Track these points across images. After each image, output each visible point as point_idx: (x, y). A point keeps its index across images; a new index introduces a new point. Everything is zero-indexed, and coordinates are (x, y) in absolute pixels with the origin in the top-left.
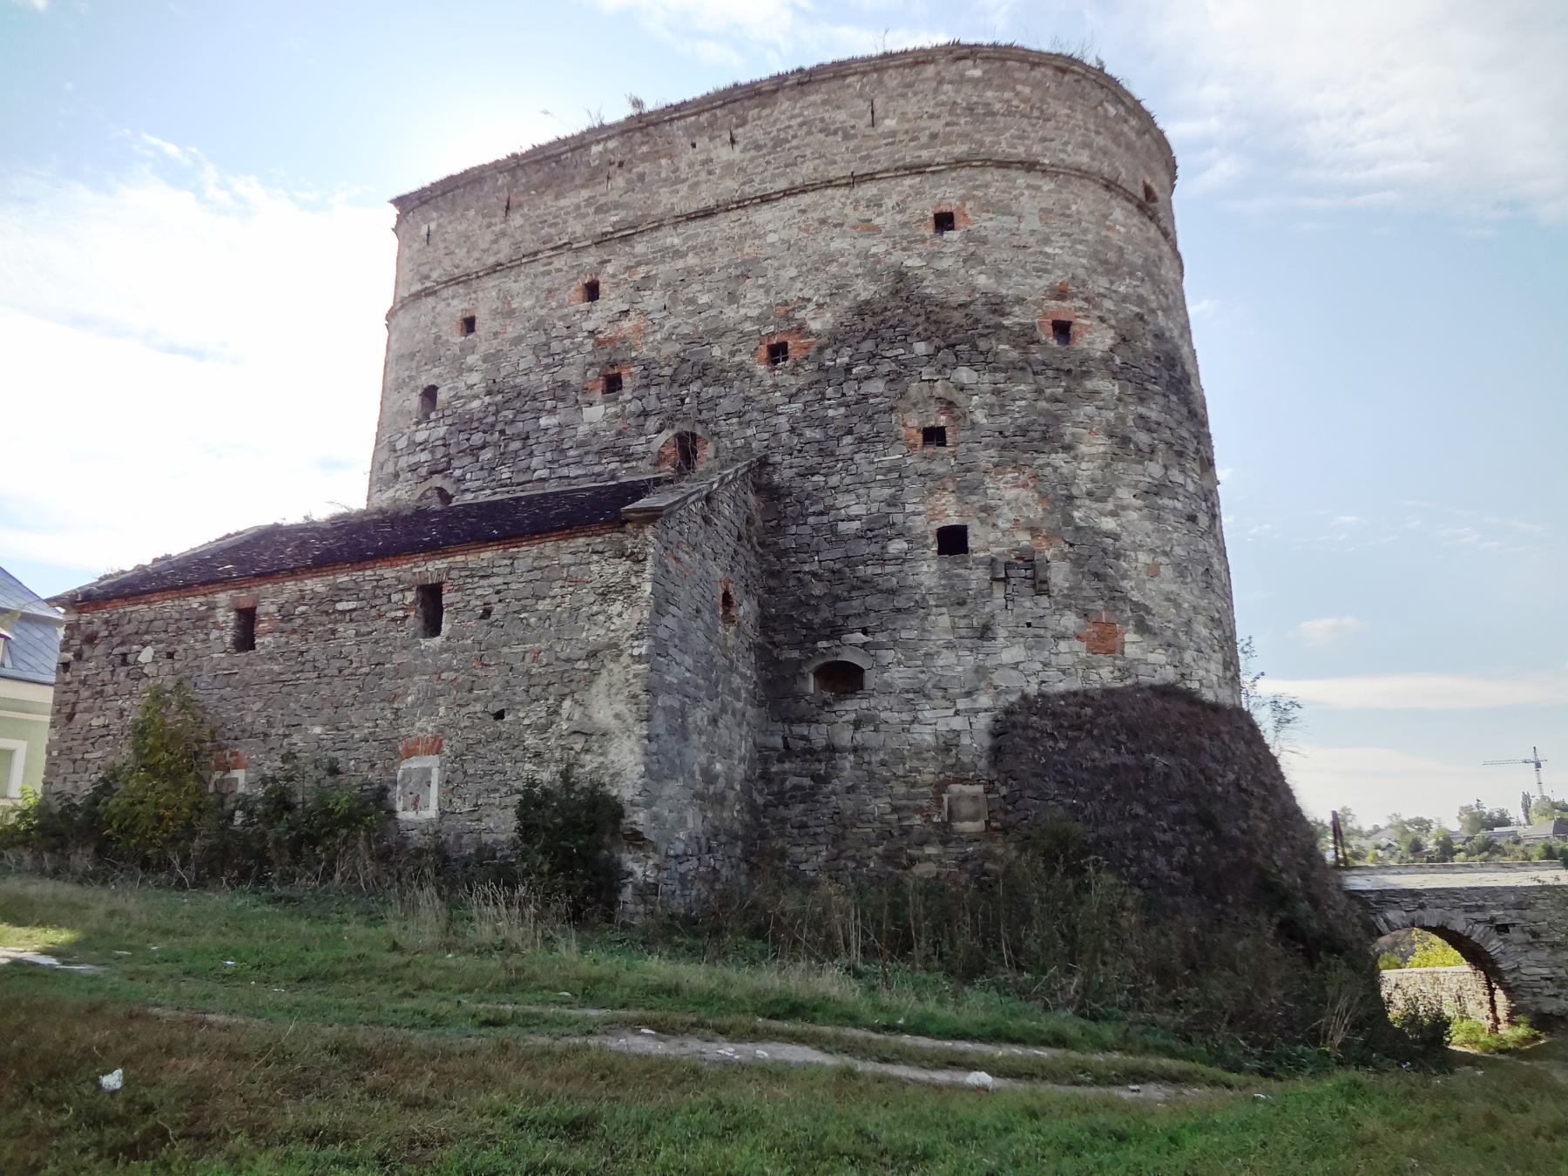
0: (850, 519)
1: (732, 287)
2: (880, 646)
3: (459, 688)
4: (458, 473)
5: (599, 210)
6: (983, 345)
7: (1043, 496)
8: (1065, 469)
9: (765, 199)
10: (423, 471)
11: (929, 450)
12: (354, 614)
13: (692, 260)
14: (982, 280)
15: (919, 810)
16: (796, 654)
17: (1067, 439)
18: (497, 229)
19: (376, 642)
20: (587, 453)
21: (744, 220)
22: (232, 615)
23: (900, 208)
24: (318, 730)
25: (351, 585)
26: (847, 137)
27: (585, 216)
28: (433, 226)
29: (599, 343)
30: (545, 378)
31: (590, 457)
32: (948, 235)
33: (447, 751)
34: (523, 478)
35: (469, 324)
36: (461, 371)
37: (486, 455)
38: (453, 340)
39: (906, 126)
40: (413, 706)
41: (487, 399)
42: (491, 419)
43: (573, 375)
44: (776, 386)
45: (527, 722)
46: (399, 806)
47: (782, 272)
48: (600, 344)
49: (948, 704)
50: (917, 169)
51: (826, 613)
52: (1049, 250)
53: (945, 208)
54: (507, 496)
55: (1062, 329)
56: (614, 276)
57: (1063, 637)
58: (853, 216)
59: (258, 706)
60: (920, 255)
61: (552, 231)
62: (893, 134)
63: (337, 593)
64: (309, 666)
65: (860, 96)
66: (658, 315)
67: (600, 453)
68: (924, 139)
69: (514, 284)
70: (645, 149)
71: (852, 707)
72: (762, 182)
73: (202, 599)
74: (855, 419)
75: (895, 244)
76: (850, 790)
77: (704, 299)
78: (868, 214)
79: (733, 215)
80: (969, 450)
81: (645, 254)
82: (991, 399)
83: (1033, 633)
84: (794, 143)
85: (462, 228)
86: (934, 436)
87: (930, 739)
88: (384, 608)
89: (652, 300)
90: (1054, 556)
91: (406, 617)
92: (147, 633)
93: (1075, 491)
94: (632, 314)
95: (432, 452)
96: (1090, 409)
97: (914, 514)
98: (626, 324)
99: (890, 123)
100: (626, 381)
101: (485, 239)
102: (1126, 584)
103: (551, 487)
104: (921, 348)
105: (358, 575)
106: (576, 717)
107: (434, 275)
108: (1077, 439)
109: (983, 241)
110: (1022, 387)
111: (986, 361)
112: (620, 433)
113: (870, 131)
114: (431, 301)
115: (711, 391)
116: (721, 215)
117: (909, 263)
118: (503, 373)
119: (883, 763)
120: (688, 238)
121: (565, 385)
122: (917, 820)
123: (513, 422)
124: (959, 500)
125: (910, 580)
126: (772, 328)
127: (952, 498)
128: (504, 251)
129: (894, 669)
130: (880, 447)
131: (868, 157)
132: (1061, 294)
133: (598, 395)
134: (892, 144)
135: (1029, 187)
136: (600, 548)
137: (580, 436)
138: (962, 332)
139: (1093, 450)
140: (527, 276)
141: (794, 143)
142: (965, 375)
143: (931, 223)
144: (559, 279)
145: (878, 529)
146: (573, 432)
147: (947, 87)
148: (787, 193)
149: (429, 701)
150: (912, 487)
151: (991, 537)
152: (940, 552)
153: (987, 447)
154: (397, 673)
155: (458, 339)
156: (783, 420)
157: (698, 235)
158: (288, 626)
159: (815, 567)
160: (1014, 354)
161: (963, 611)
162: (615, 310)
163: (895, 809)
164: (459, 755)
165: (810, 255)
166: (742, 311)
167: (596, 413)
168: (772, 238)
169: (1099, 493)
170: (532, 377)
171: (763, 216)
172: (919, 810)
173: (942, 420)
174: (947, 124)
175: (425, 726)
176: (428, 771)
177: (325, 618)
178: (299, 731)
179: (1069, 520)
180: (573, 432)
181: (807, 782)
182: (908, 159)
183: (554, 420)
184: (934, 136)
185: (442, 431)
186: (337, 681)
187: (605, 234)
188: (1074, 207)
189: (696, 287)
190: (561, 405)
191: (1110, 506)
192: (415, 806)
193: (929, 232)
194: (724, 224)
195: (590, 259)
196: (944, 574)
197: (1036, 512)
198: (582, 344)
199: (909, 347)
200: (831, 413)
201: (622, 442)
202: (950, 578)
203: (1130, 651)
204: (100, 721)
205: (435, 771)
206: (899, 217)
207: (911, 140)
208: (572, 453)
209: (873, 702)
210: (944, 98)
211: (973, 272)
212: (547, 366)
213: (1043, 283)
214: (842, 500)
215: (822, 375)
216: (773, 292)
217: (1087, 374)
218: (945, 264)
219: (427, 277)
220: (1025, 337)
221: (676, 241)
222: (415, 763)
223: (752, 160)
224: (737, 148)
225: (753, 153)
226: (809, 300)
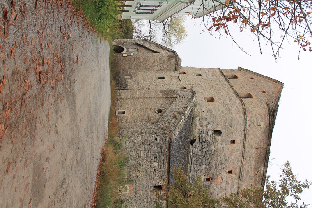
5: (248, 171)
10: (201, 136)
20: (194, 176)
22: (161, 185)
27: (248, 168)
29: (217, 176)
30: (214, 165)
35: (233, 142)
37: (200, 153)
43: (213, 171)
54: (189, 160)
59: (142, 194)
61: (248, 160)
64: (148, 204)
69: (238, 154)
73: (166, 177)
89: (224, 184)
92: (161, 163)
98: (220, 179)
101: (252, 143)
107: (249, 129)
133: (206, 177)
140: (239, 156)
146: (200, 173)
155: (231, 139)
183: (203, 168)
185: (209, 139)
198: (219, 172)
204: (142, 154)
208: (195, 173)
212: (216, 165)
219: (250, 126)
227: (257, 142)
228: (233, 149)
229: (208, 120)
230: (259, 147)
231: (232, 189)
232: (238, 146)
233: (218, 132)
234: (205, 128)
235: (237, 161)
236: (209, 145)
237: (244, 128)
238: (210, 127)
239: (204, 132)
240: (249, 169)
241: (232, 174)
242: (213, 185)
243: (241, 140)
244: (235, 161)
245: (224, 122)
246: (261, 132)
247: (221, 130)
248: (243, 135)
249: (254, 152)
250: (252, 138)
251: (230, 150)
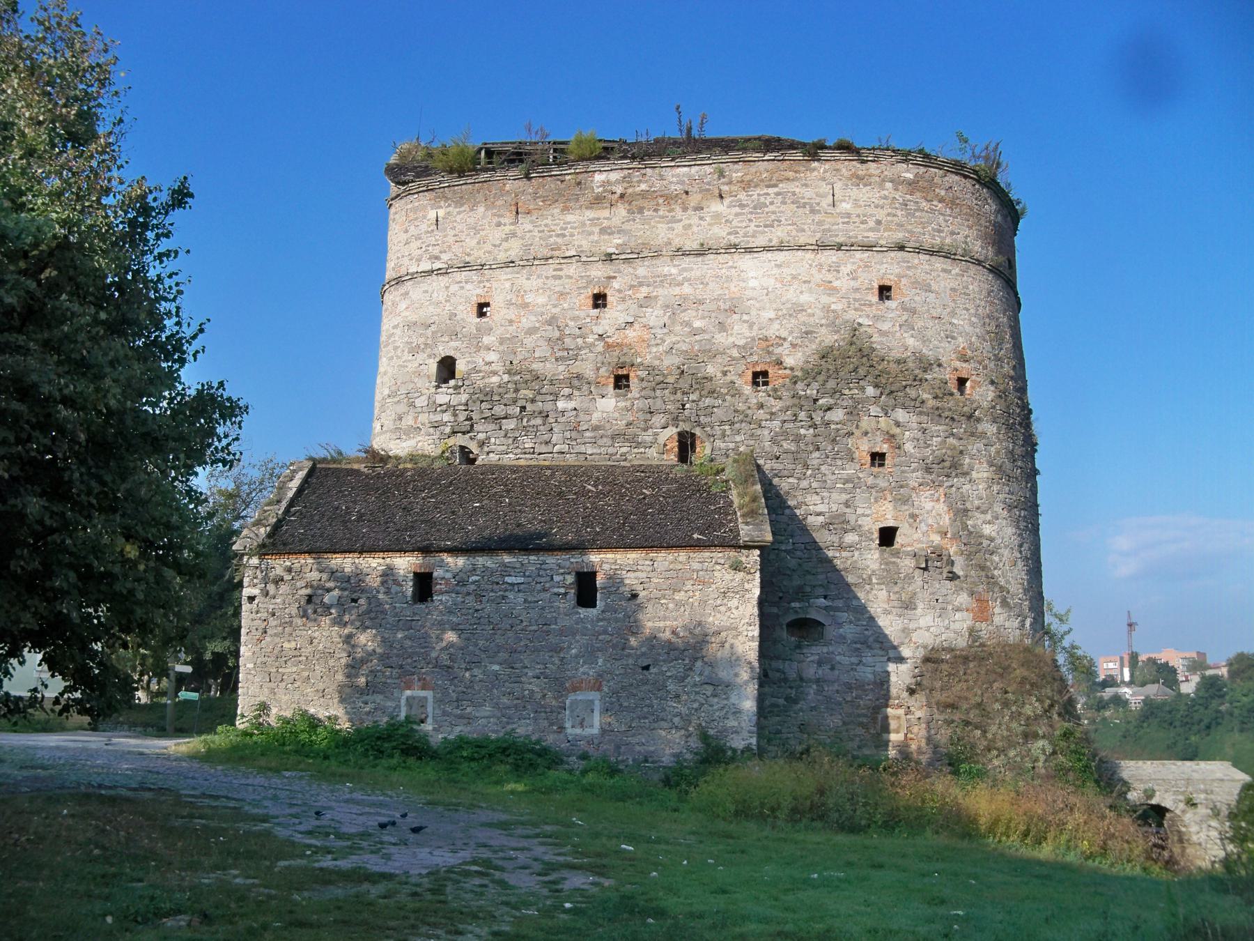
0: (819, 514)
1: (722, 318)
2: (837, 609)
3: (614, 647)
4: (481, 436)
5: (603, 231)
7: (950, 507)
9: (749, 250)
10: (448, 430)
11: (876, 470)
12: (522, 587)
13: (687, 289)
14: (911, 342)
15: (861, 724)
16: (775, 610)
17: (966, 467)
18: (508, 229)
19: (543, 608)
21: (730, 264)
23: (853, 276)
24: (496, 667)
25: (518, 565)
26: (813, 211)
27: (593, 233)
28: (441, 213)
29: (608, 346)
31: (605, 440)
32: (888, 303)
33: (606, 689)
34: (544, 449)
36: (478, 349)
37: (509, 425)
38: (469, 320)
39: (859, 211)
40: (577, 656)
41: (506, 378)
42: (511, 395)
44: (761, 406)
45: (669, 674)
46: (568, 725)
47: (762, 313)
48: (608, 346)
49: (881, 653)
50: (868, 247)
51: (797, 582)
52: (955, 321)
55: (962, 382)
56: (619, 291)
57: (958, 610)
58: (818, 277)
60: (868, 316)
61: (559, 240)
62: (849, 215)
63: (506, 569)
65: (824, 179)
66: (659, 331)
67: (613, 438)
68: (872, 224)
70: (643, 187)
71: (814, 653)
72: (745, 235)
73: (381, 561)
74: (821, 439)
75: (849, 303)
76: (812, 709)
77: (697, 324)
78: (829, 277)
80: (903, 472)
81: (645, 277)
83: (941, 607)
84: (772, 208)
85: (471, 221)
86: (877, 458)
87: (871, 676)
88: (547, 585)
89: (654, 316)
90: (956, 553)
91: (566, 594)
93: (968, 505)
94: (636, 326)
95: (455, 415)
97: (864, 515)
98: (631, 334)
99: (845, 206)
100: (633, 382)
101: (497, 235)
102: (996, 573)
103: (571, 459)
104: (870, 391)
105: (523, 559)
106: (706, 673)
107: (445, 257)
109: (913, 312)
110: (941, 428)
111: (917, 405)
112: (629, 424)
113: (830, 209)
115: (708, 401)
117: (860, 320)
118: (520, 357)
119: (837, 692)
120: (685, 270)
121: (579, 377)
122: (860, 731)
123: (533, 401)
124: (895, 508)
125: (859, 565)
126: (755, 358)
127: (890, 506)
128: (514, 249)
129: (847, 626)
130: (839, 463)
134: (848, 223)
135: (944, 270)
136: (722, 561)
137: (594, 422)
138: (896, 381)
139: (980, 475)
141: (772, 208)
142: (900, 415)
143: (877, 292)
144: (568, 285)
145: (838, 523)
146: (588, 418)
147: (889, 185)
148: (767, 249)
149: (589, 655)
150: (860, 495)
151: (916, 536)
152: (880, 545)
153: (913, 471)
154: (562, 633)
156: (766, 432)
157: (692, 269)
158: (464, 589)
159: (790, 547)
160: (931, 403)
161: (896, 589)
163: (844, 723)
164: (615, 692)
166: (731, 340)
167: (608, 405)
168: (753, 283)
169: (983, 508)
170: (548, 365)
171: (746, 263)
172: (861, 724)
173: (885, 448)
174: (889, 215)
175: (586, 671)
176: (592, 702)
177: (495, 587)
178: (479, 667)
179: (965, 527)
180: (588, 418)
181: (781, 701)
182: (860, 238)
183: (571, 405)
184: (879, 222)
185: (464, 397)
186: (510, 634)
189: (691, 313)
190: (576, 393)
191: (989, 517)
192: (582, 725)
193: (875, 299)
196: (883, 561)
197: (946, 520)
198: (593, 345)
200: (802, 431)
201: (631, 431)
202: (887, 564)
203: (998, 620)
204: (293, 645)
205: (597, 703)
206: (852, 283)
207: (862, 223)
208: (588, 434)
209: (831, 649)
210: (886, 192)
211: (905, 335)
214: (811, 498)
215: (796, 401)
216: (755, 327)
217: (979, 420)
218: (885, 326)
219: (437, 258)
221: (674, 271)
222: (580, 696)
223: (737, 215)
224: (727, 201)
225: (737, 210)
226: (785, 339)
227: (496, 220)
228: (510, 304)
229: (402, 408)
230: (514, 208)
231: (680, 278)
232: (500, 289)
233: (447, 368)
234: (424, 418)
235: (557, 282)
236: (487, 396)
237: (441, 278)
238: (421, 402)
239: (438, 417)
240: (597, 230)
241: (606, 291)
242: (648, 359)
243: (480, 282)
244: (557, 289)
245: (414, 350)
246: (459, 213)
247: (438, 359)
248: (464, 275)
249: (532, 222)
250: (478, 243)
251: (512, 314)
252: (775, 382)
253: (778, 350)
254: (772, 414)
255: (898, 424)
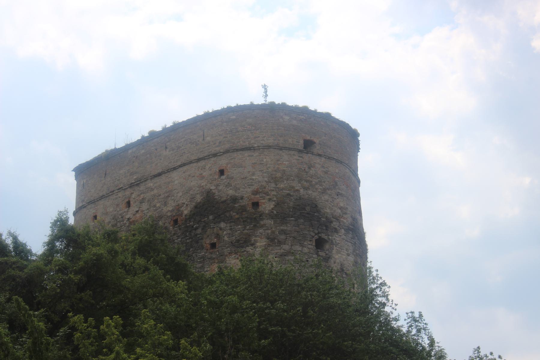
6: (228, 214)
8: (251, 251)
13: (155, 191)
17: (252, 242)
52: (254, 177)
53: (222, 168)
55: (256, 205)
56: (134, 199)
68: (217, 144)
77: (158, 205)
79: (166, 175)
82: (229, 232)
84: (183, 148)
86: (213, 246)
89: (145, 206)
96: (261, 231)
97: (207, 271)
98: (138, 215)
108: (256, 241)
110: (240, 227)
114: (85, 210)
116: (163, 175)
131: (202, 151)
132: (256, 193)
135: (249, 156)
139: (261, 244)
142: (222, 225)
148: (180, 166)
162: (135, 210)
165: (183, 189)
174: (224, 138)
187: (132, 183)
188: (265, 160)
194: (163, 177)
195: (128, 193)
198: (125, 224)
199: (208, 218)
200: (188, 241)
213: (249, 190)
218: (220, 188)
220: (243, 209)
221: (152, 185)
224: (168, 150)
225: (172, 152)
226: (184, 203)
252: (180, 222)
253: (182, 209)
254: (178, 236)
255: (221, 229)
